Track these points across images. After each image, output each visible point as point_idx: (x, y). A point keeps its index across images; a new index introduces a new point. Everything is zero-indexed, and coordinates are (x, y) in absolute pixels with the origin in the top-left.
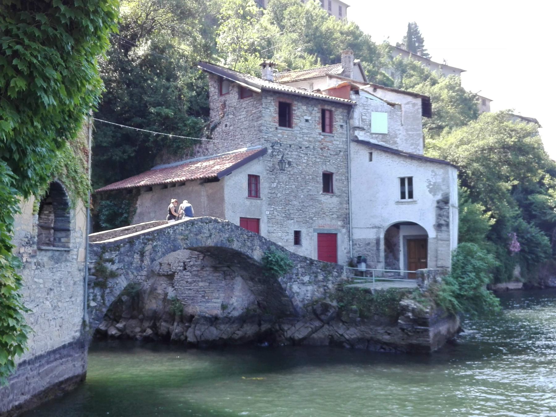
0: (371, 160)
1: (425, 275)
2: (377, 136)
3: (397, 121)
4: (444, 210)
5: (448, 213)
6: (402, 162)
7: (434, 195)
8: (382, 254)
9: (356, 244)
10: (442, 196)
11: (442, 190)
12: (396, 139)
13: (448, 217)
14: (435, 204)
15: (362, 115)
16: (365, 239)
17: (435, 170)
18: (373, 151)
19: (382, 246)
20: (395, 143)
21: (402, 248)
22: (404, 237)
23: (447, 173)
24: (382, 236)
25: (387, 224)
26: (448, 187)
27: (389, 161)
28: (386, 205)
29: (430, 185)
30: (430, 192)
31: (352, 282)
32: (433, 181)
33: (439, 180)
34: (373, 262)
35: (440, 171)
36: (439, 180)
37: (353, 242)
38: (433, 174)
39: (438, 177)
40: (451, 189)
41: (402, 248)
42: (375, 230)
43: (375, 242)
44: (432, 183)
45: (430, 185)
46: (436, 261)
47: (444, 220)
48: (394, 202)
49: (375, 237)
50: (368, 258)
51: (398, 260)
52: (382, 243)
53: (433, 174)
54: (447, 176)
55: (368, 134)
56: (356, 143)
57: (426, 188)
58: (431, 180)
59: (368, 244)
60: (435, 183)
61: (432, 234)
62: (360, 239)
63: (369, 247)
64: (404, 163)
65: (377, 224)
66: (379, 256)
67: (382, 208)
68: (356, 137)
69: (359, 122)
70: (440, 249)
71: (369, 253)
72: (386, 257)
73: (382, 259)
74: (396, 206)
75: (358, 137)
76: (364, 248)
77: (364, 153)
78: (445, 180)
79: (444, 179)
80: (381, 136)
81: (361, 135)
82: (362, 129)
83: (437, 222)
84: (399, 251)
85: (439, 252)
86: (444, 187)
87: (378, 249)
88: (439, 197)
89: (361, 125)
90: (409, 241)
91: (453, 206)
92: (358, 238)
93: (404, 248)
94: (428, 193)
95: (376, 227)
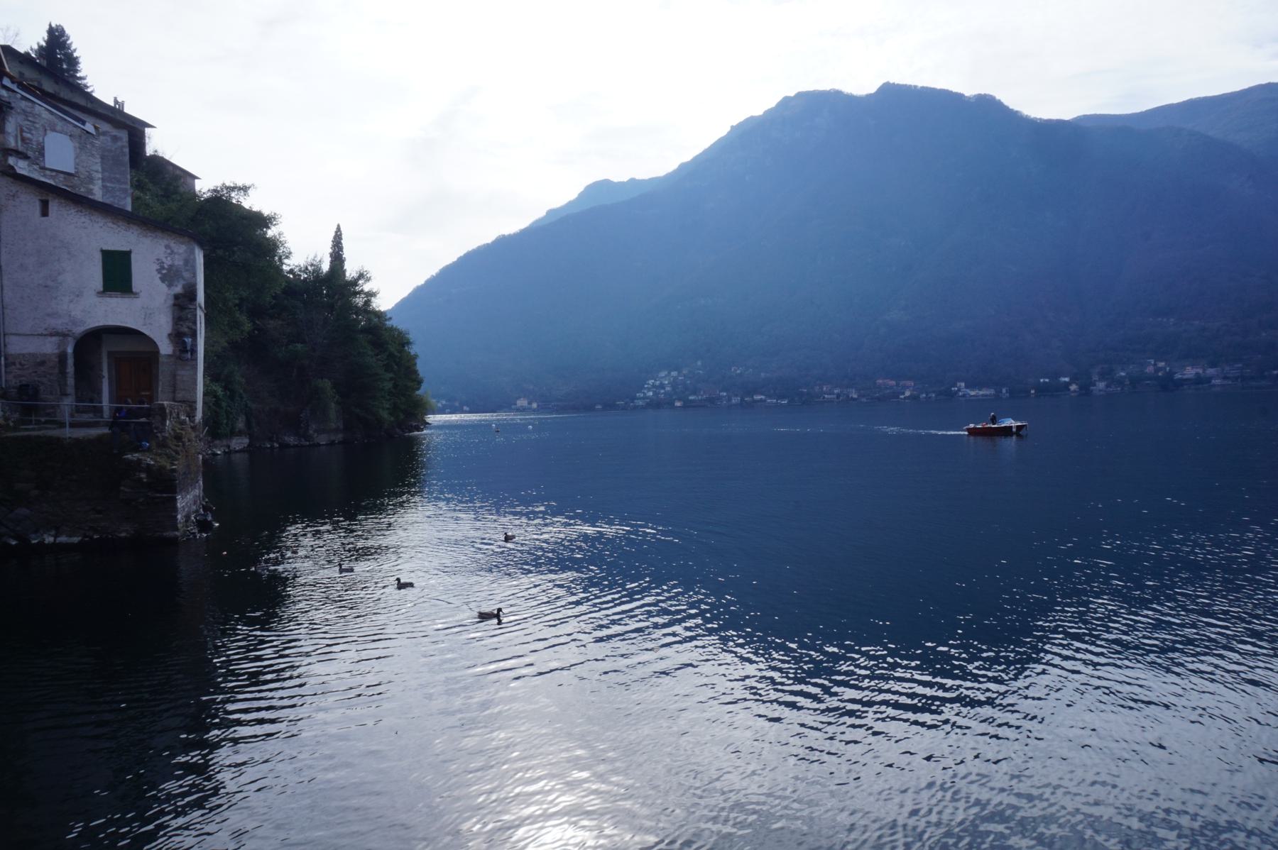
0: (45, 213)
1: (167, 411)
2: (54, 174)
3: (93, 155)
4: (187, 311)
5: (196, 315)
6: (110, 225)
7: (170, 286)
8: (71, 381)
9: (14, 364)
10: (184, 287)
11: (184, 279)
12: (91, 187)
13: (195, 323)
14: (171, 302)
15: (22, 131)
16: (33, 355)
17: (172, 245)
18: (50, 198)
19: (70, 369)
20: (90, 191)
21: (105, 373)
22: (110, 354)
23: (192, 252)
24: (70, 350)
25: (79, 330)
26: (194, 275)
27: (83, 219)
28: (78, 296)
29: (163, 268)
30: (163, 279)
31: (15, 429)
32: (168, 262)
33: (179, 262)
34: (51, 394)
35: (181, 248)
36: (179, 262)
37: (6, 359)
38: (169, 251)
39: (177, 256)
40: (198, 280)
41: (105, 373)
42: (54, 339)
43: (57, 360)
44: (166, 266)
45: (163, 268)
46: (174, 392)
47: (188, 327)
49: (56, 351)
50: (42, 388)
51: (100, 393)
52: (70, 361)
53: (169, 251)
54: (192, 257)
55: (36, 167)
56: (12, 180)
57: (156, 273)
58: (164, 260)
59: (42, 363)
60: (171, 266)
61: (165, 348)
62: (24, 355)
63: (42, 368)
64: (115, 226)
66: (66, 384)
67: (71, 301)
68: (12, 168)
69: (16, 142)
70: (179, 372)
72: (77, 387)
73: (70, 389)
74: (100, 299)
75: (16, 168)
77: (28, 203)
78: (190, 263)
79: (187, 262)
80: (62, 175)
81: (22, 167)
82: (25, 157)
83: (174, 329)
84: (101, 377)
85: (178, 378)
86: (187, 275)
87: (63, 372)
88: (178, 289)
89: (20, 149)
90: (118, 361)
91: (201, 308)
92: (18, 352)
93: (109, 372)
94: (159, 282)
95: (56, 334)
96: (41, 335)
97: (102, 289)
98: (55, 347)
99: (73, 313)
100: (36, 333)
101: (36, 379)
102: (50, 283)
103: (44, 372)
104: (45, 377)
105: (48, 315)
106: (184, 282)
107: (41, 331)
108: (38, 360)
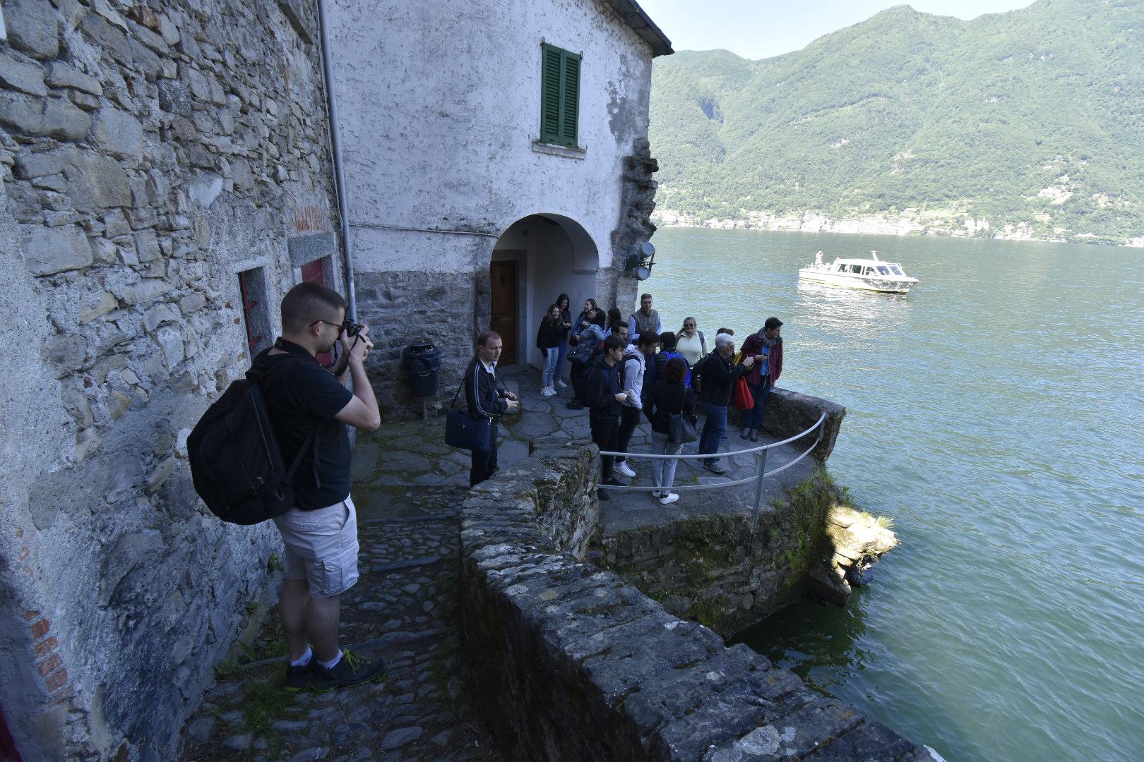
7: (620, 140)
9: (371, 294)
10: (635, 147)
14: (619, 172)
25: (506, 223)
34: (457, 355)
42: (466, 242)
43: (469, 286)
48: (528, 143)
49: (470, 269)
59: (438, 293)
62: (395, 276)
65: (476, 218)
71: (438, 327)
76: (411, 308)
92: (383, 269)
96: (437, 231)
97: (538, 136)
98: (468, 260)
99: (495, 186)
100: (424, 227)
101: (423, 326)
102: (450, 107)
103: (442, 311)
104: (444, 321)
105: (450, 186)
106: (636, 137)
107: (435, 222)
108: (428, 288)
